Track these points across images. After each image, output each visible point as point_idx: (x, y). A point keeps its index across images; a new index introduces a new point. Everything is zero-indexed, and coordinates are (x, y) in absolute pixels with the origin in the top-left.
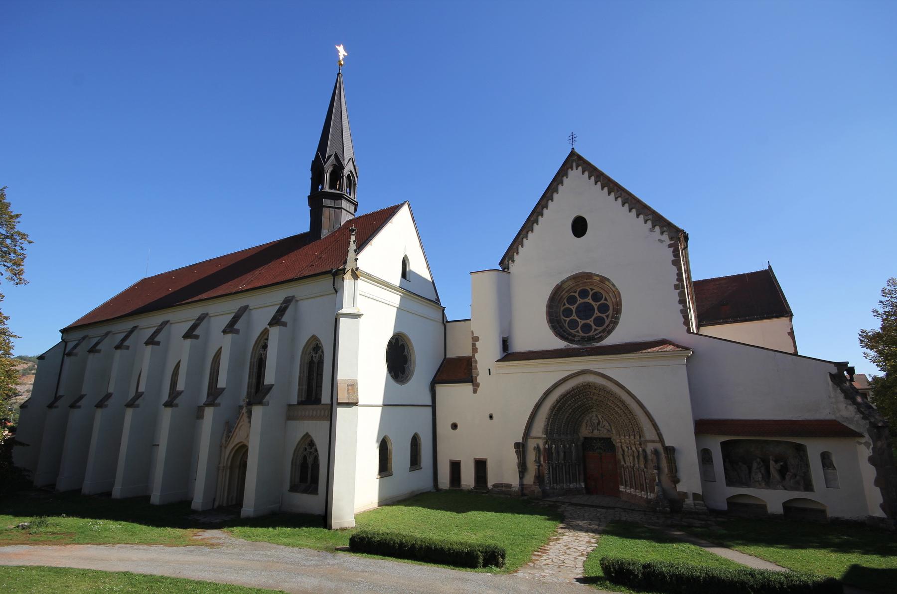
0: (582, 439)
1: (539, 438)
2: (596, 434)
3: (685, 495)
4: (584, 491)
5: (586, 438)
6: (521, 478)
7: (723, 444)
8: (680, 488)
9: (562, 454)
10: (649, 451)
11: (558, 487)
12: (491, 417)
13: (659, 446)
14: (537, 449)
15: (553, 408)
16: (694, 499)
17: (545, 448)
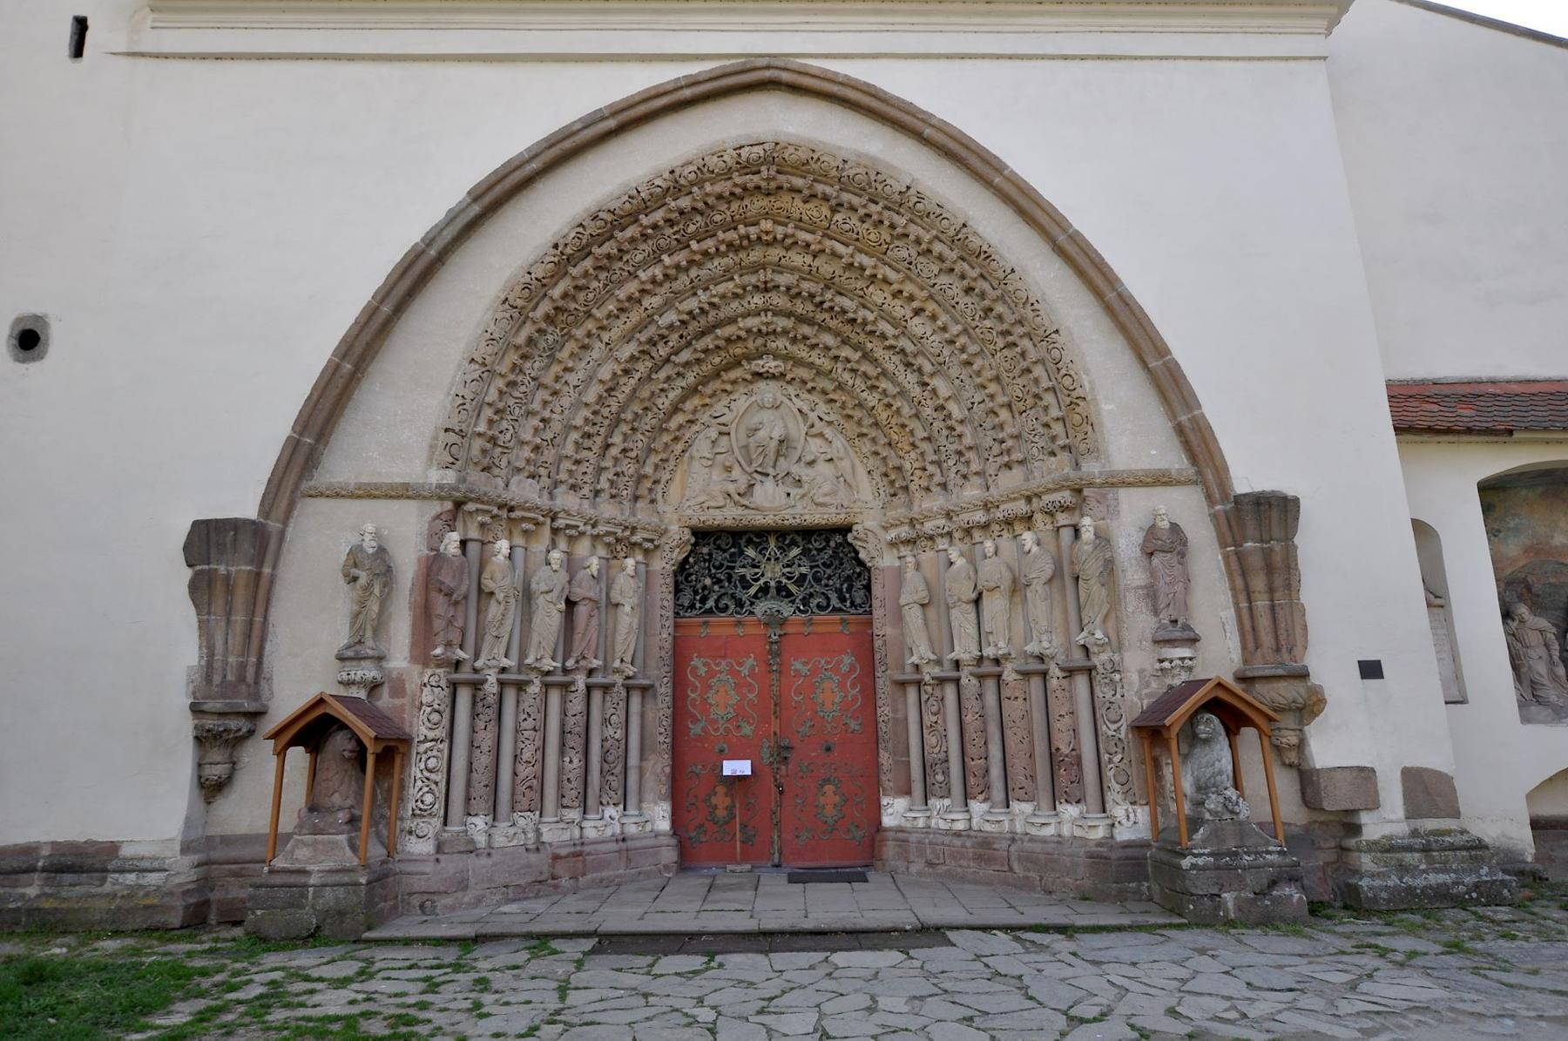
1: (403, 492)
2: (772, 504)
3: (1365, 775)
4: (669, 855)
5: (702, 535)
6: (211, 789)
7: (1493, 492)
8: (1328, 748)
9: (548, 618)
10: (1127, 543)
11: (503, 836)
12: (29, 340)
13: (1185, 508)
14: (369, 569)
15: (535, 289)
16: (1412, 812)
17: (433, 564)
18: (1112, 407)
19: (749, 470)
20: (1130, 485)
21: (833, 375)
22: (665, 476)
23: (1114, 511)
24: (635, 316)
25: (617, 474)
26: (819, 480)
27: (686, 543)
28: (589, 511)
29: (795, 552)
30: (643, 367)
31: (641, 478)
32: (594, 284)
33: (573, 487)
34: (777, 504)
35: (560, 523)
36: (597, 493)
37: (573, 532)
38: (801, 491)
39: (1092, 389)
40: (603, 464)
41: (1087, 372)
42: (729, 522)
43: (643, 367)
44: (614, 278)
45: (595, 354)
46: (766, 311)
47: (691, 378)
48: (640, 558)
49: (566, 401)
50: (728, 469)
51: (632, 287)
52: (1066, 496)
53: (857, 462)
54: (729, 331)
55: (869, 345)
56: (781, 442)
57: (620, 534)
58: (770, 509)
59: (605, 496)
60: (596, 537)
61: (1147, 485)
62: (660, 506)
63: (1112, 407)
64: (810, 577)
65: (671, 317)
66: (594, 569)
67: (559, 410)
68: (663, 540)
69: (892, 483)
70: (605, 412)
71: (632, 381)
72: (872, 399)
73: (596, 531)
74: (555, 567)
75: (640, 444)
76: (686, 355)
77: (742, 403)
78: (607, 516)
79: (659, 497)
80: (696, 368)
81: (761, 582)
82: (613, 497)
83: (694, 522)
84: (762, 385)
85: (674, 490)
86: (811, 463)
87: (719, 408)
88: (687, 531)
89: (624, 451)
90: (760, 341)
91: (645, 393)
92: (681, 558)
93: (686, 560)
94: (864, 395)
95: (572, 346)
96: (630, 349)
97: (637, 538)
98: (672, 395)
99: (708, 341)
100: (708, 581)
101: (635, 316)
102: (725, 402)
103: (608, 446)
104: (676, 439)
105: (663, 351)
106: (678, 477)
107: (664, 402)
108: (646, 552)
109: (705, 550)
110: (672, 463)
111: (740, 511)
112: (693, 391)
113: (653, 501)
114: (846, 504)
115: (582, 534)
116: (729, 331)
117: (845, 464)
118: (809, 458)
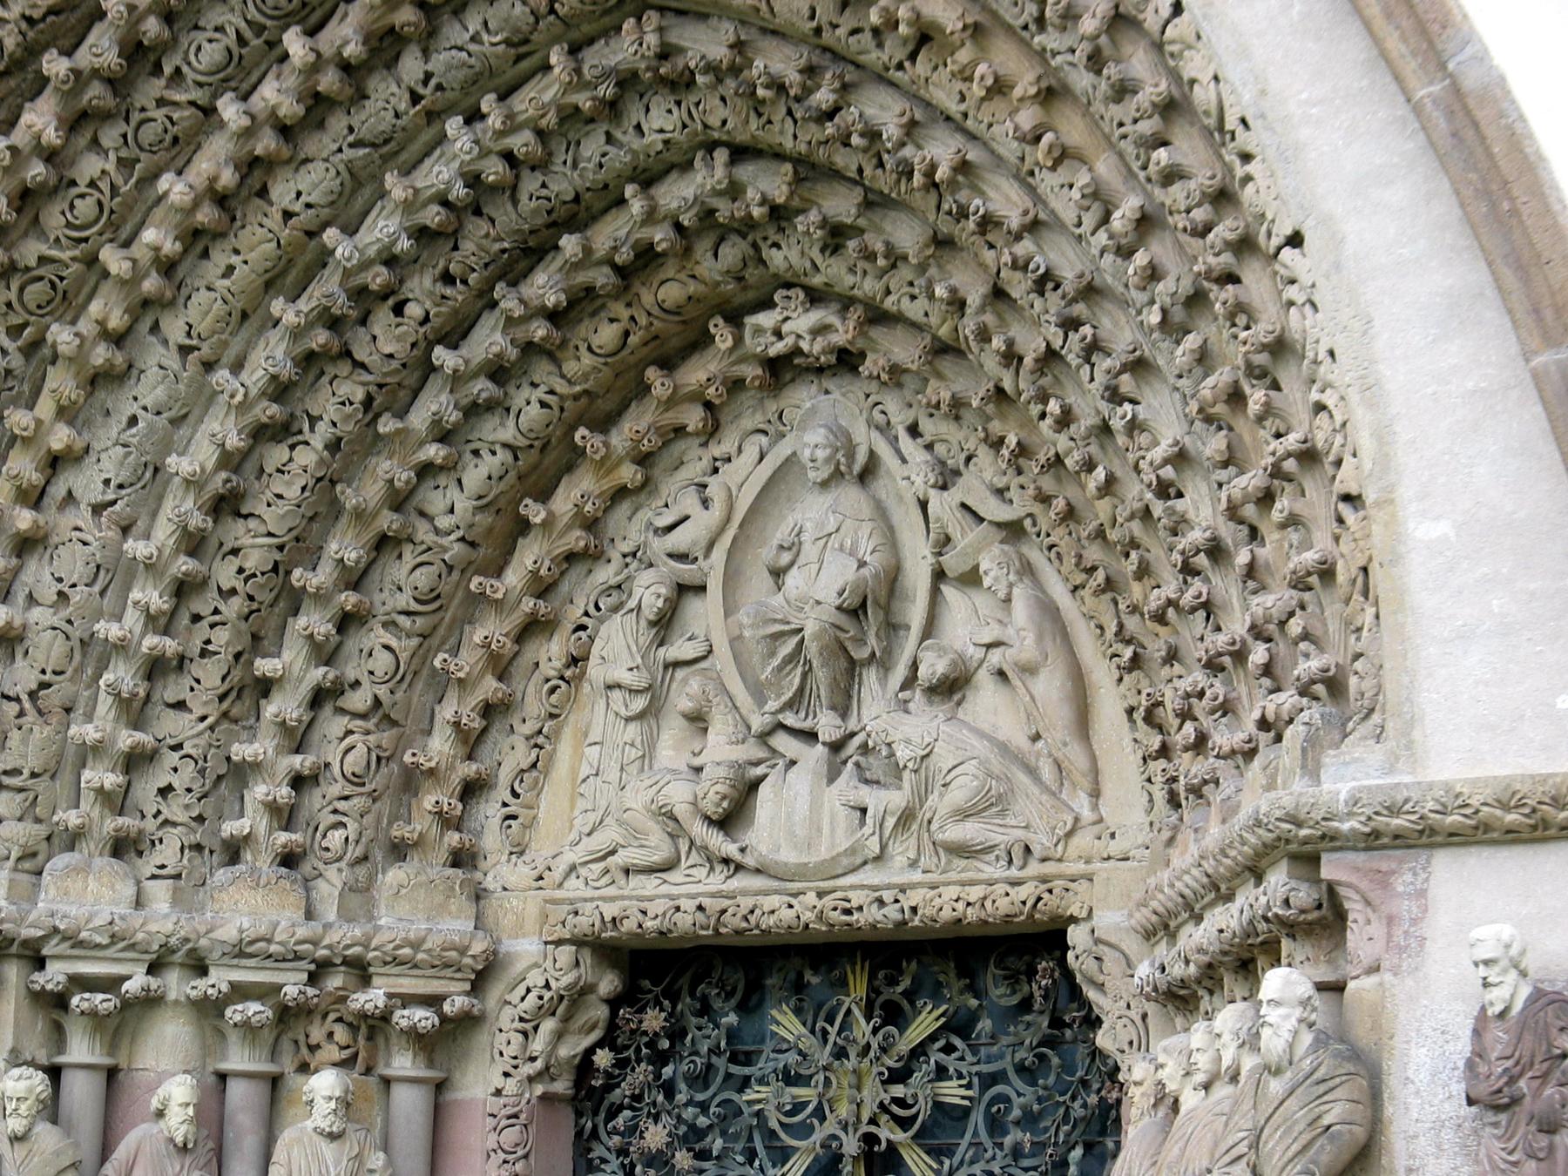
0: (535, 961)
2: (815, 851)
18: (1442, 528)
19: (758, 722)
20: (1457, 838)
22: (509, 754)
23: (1405, 944)
24: (256, 243)
25: (298, 782)
26: (944, 758)
27: (579, 995)
28: (162, 918)
29: (925, 1023)
30: (333, 403)
31: (412, 780)
32: (90, 166)
33: (123, 847)
34: (823, 852)
35: (54, 976)
36: (233, 851)
37: (101, 1001)
38: (896, 799)
39: (1384, 461)
40: (242, 751)
41: (1370, 388)
42: (684, 921)
43: (333, 403)
44: (149, 134)
45: (150, 389)
46: (711, 147)
47: (529, 408)
48: (403, 1063)
49: (71, 562)
50: (698, 720)
51: (214, 161)
52: (1278, 879)
53: (1101, 674)
54: (613, 233)
56: (856, 612)
57: (293, 985)
58: (800, 873)
59: (261, 861)
60: (209, 1010)
61: (1512, 837)
62: (500, 872)
63: (1442, 528)
64: (977, 1118)
65: (383, 228)
66: (178, 1123)
67: (48, 592)
68: (495, 992)
70: (225, 573)
71: (306, 458)
73: (201, 987)
74: (15, 1125)
75: (382, 662)
76: (489, 340)
77: (745, 473)
78: (228, 933)
79: (492, 840)
80: (542, 370)
81: (818, 1136)
82: (289, 860)
83: (585, 923)
84: (803, 397)
85: (551, 803)
86: (951, 687)
87: (676, 494)
88: (566, 954)
89: (318, 698)
90: (732, 252)
91: (364, 491)
92: (571, 1049)
93: (585, 1066)
95: (61, 383)
96: (271, 356)
97: (372, 998)
98: (475, 475)
99: (545, 286)
100: (655, 1136)
101: (256, 243)
102: (695, 469)
103: (265, 687)
104: (533, 628)
105: (386, 338)
106: (564, 749)
107: (453, 505)
108: (422, 1042)
109: (653, 1020)
110: (534, 705)
111: (717, 881)
112: (544, 465)
113: (462, 859)
114: (1041, 841)
115: (150, 1002)
116: (613, 233)
117: (1049, 687)
118: (933, 666)
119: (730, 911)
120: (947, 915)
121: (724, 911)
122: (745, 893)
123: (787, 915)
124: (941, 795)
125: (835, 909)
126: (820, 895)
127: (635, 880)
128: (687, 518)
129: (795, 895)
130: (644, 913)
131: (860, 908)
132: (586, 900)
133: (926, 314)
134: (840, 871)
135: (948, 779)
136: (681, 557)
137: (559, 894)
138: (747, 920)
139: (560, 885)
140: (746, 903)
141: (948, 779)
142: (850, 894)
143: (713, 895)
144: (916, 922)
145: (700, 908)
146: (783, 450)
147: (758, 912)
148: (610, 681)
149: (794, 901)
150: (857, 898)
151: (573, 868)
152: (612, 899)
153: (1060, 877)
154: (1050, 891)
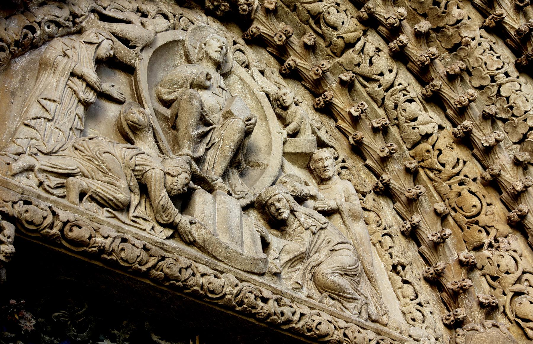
21: (350, 54)
55: (456, 12)
58: (234, 259)
69: (454, 297)
72: (430, 119)
94: (414, 108)
111: (161, 235)
119: (170, 260)
120: (324, 328)
121: (163, 258)
122: (181, 253)
123: (216, 283)
124: (328, 256)
125: (251, 292)
126: (241, 280)
127: (87, 205)
128: (129, 22)
129: (222, 272)
130: (97, 231)
131: (265, 300)
132: (39, 197)
133: (343, 23)
134: (256, 271)
135: (337, 247)
136: (126, 41)
137: (10, 180)
138: (180, 272)
139: (14, 175)
140: (184, 262)
141: (337, 247)
142: (262, 289)
143: (155, 244)
144: (299, 325)
145: (145, 249)
146: (179, 35)
147: (190, 271)
148: (78, 71)
149: (219, 275)
150: (266, 294)
151: (31, 169)
152: (65, 208)
153: (388, 334)
154: (382, 340)
